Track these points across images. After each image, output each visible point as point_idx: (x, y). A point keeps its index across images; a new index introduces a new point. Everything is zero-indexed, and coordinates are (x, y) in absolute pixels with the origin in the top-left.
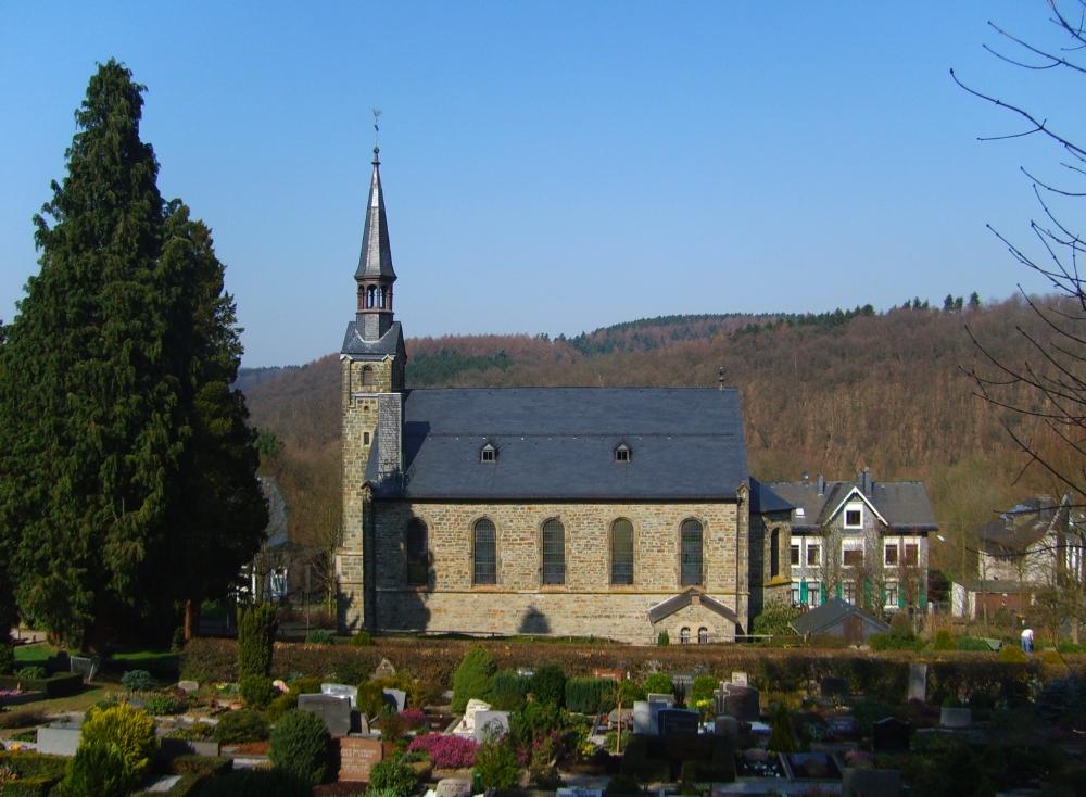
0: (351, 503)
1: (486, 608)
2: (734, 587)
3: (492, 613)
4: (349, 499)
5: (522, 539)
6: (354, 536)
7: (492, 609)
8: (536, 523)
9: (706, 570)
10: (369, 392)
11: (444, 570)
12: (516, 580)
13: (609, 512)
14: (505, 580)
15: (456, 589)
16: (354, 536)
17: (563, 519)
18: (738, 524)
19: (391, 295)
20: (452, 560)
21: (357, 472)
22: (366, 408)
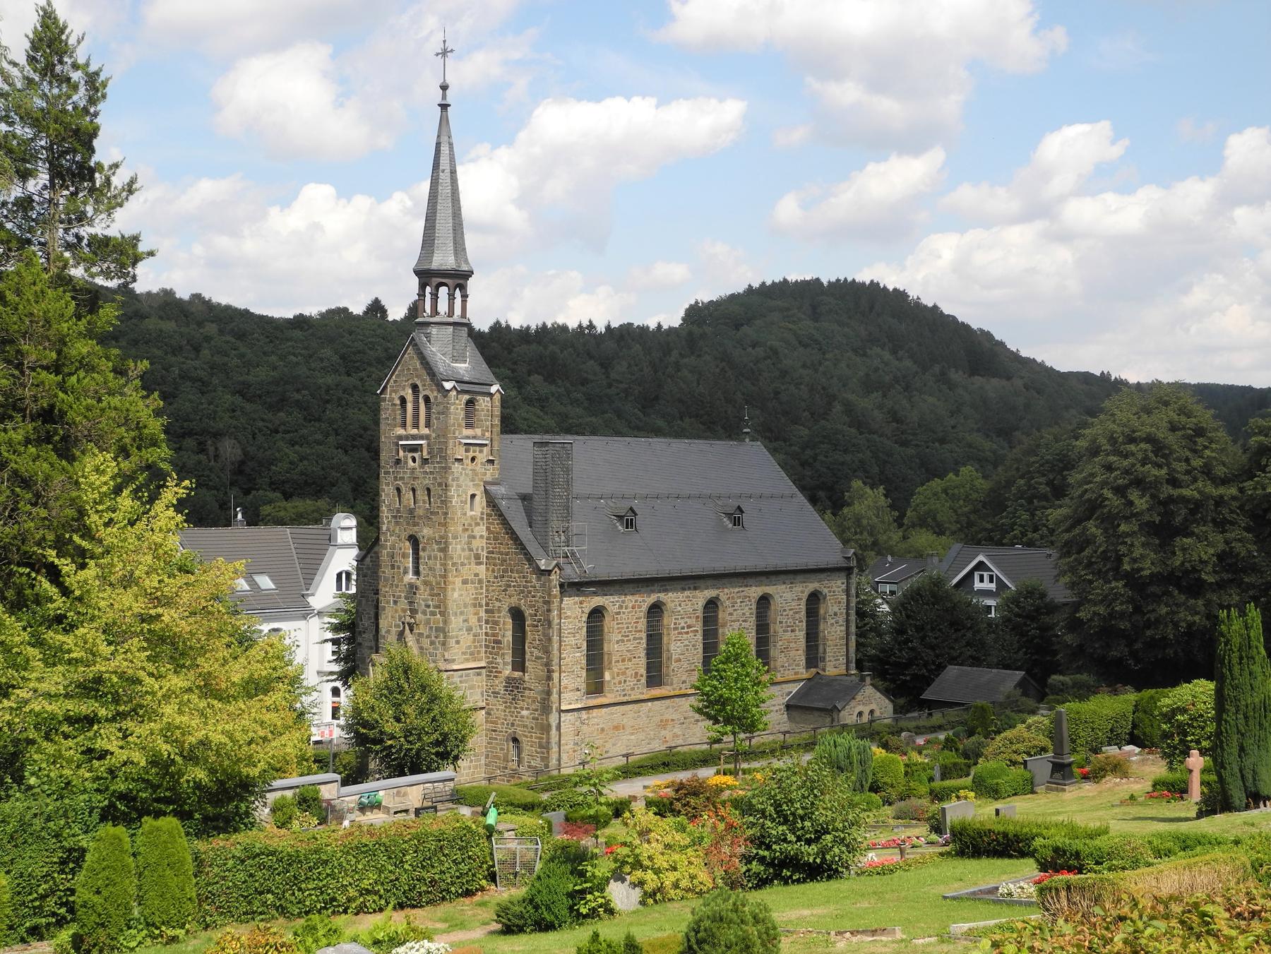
0: (456, 595)
1: (659, 718)
2: (844, 667)
3: (663, 724)
4: (454, 590)
5: (689, 627)
6: (458, 642)
7: (664, 718)
8: (701, 603)
9: (825, 652)
10: (474, 438)
11: (624, 673)
12: (684, 678)
13: (755, 592)
14: (675, 680)
15: (633, 698)
16: (458, 642)
17: (723, 597)
18: (848, 595)
19: (465, 297)
20: (630, 660)
21: (463, 550)
22: (473, 459)
